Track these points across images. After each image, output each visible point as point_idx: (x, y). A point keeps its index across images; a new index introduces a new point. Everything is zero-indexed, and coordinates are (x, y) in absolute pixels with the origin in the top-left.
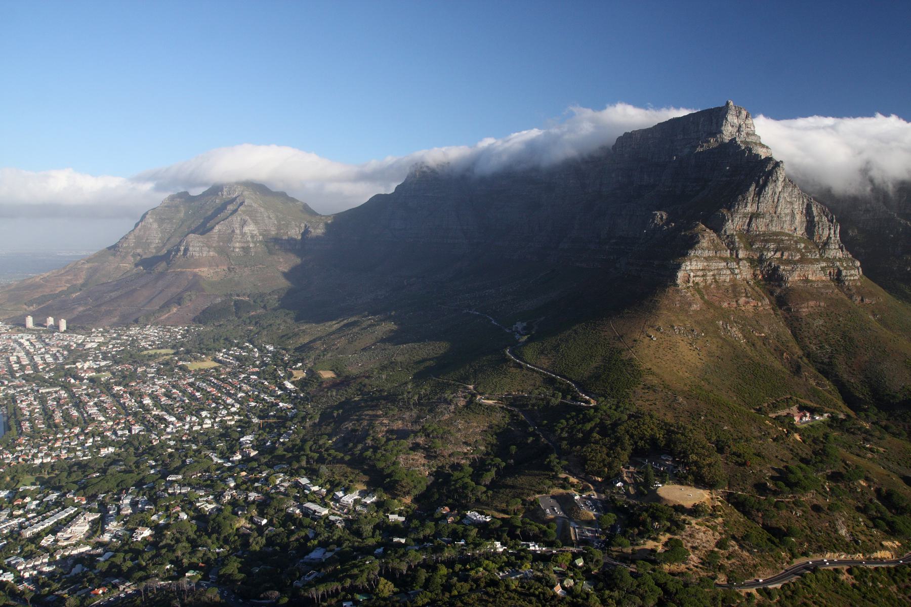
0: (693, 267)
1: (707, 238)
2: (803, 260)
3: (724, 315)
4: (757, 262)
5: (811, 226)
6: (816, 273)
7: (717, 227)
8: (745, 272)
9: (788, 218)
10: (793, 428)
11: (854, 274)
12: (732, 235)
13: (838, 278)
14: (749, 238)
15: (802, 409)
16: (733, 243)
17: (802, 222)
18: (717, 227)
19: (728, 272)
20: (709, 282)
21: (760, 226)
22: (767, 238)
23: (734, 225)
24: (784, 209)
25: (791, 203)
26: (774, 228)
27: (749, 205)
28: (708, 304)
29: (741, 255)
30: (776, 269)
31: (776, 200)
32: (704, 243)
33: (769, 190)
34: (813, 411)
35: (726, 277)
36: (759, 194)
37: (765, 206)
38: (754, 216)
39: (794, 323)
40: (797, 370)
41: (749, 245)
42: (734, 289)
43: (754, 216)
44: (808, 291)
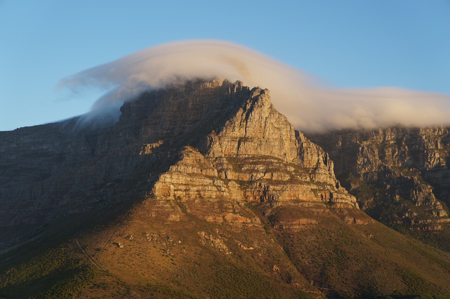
0: (174, 181)
9: (277, 143)
12: (221, 157)
16: (221, 164)
17: (292, 149)
19: (215, 189)
20: (193, 197)
21: (249, 149)
25: (279, 129)
26: (262, 152)
27: (237, 129)
29: (229, 177)
30: (266, 191)
31: (263, 125)
33: (255, 114)
41: (238, 168)
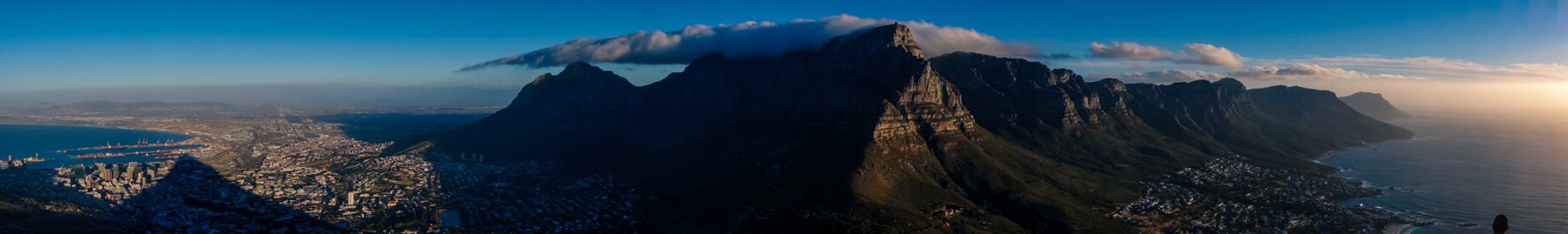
1: (890, 109)
2: (944, 119)
3: (902, 155)
4: (918, 121)
5: (946, 98)
6: (951, 127)
7: (895, 103)
8: (912, 128)
10: (945, 220)
11: (970, 125)
13: (962, 127)
14: (913, 106)
15: (949, 208)
18: (895, 103)
21: (918, 99)
22: (923, 106)
23: (904, 100)
24: (931, 89)
28: (892, 149)
32: (888, 112)
34: (955, 208)
35: (901, 132)
36: (917, 81)
37: (921, 88)
38: (916, 93)
39: (940, 155)
40: (944, 184)
42: (907, 139)
43: (916, 93)
44: (947, 136)
